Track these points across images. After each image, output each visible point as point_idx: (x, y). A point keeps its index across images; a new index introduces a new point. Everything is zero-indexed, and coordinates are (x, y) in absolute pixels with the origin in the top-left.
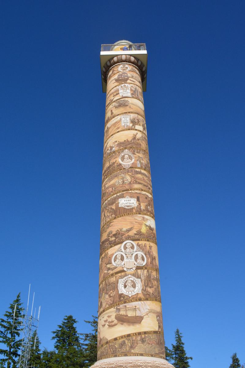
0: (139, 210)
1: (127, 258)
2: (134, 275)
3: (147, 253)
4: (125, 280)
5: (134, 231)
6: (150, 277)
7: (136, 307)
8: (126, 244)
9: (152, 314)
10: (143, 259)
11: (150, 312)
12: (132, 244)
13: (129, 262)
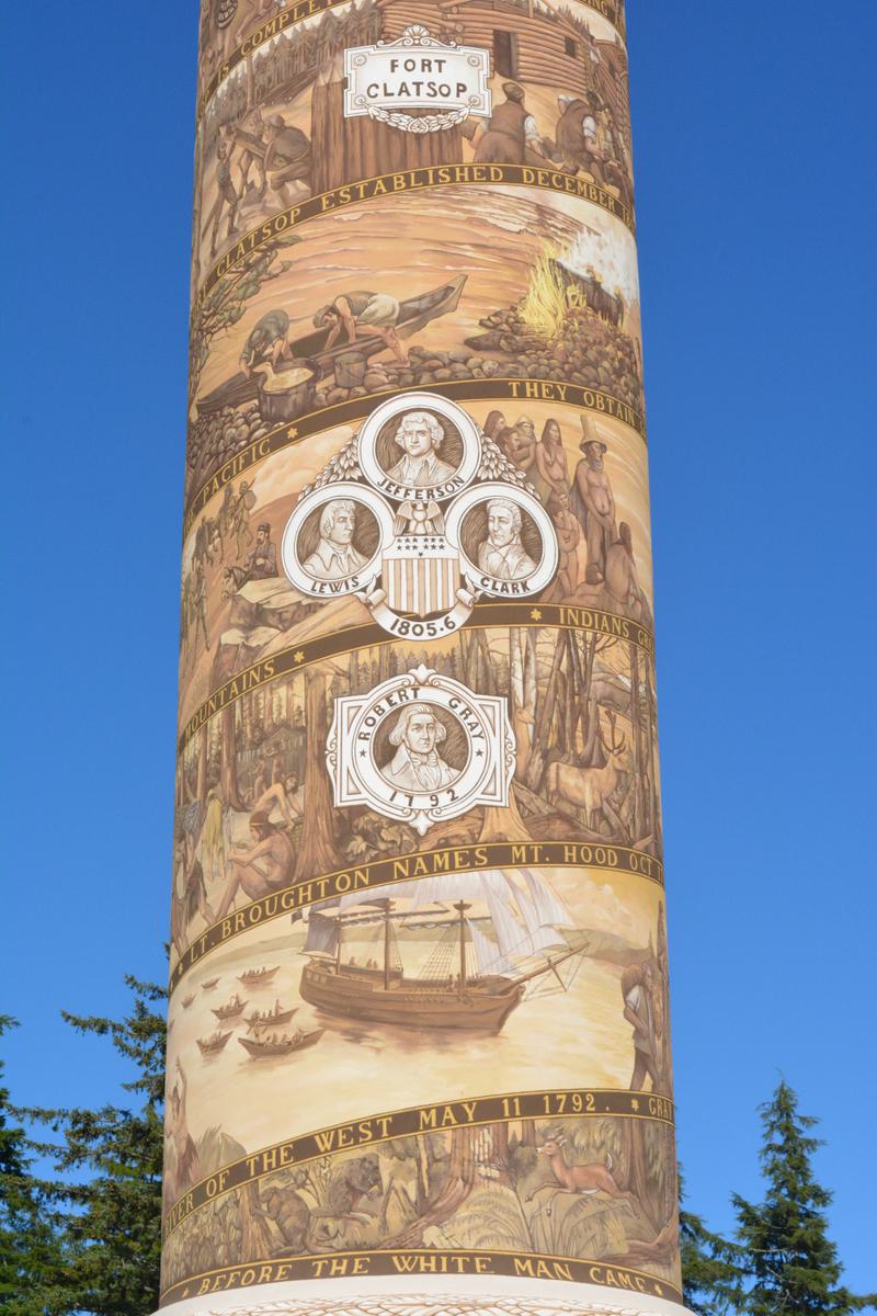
0: (510, 148)
1: (406, 530)
2: (453, 666)
3: (564, 499)
4: (384, 704)
5: (464, 321)
6: (584, 684)
7: (467, 913)
8: (396, 420)
9: (589, 962)
10: (531, 546)
11: (572, 951)
12: (442, 420)
13: (421, 568)
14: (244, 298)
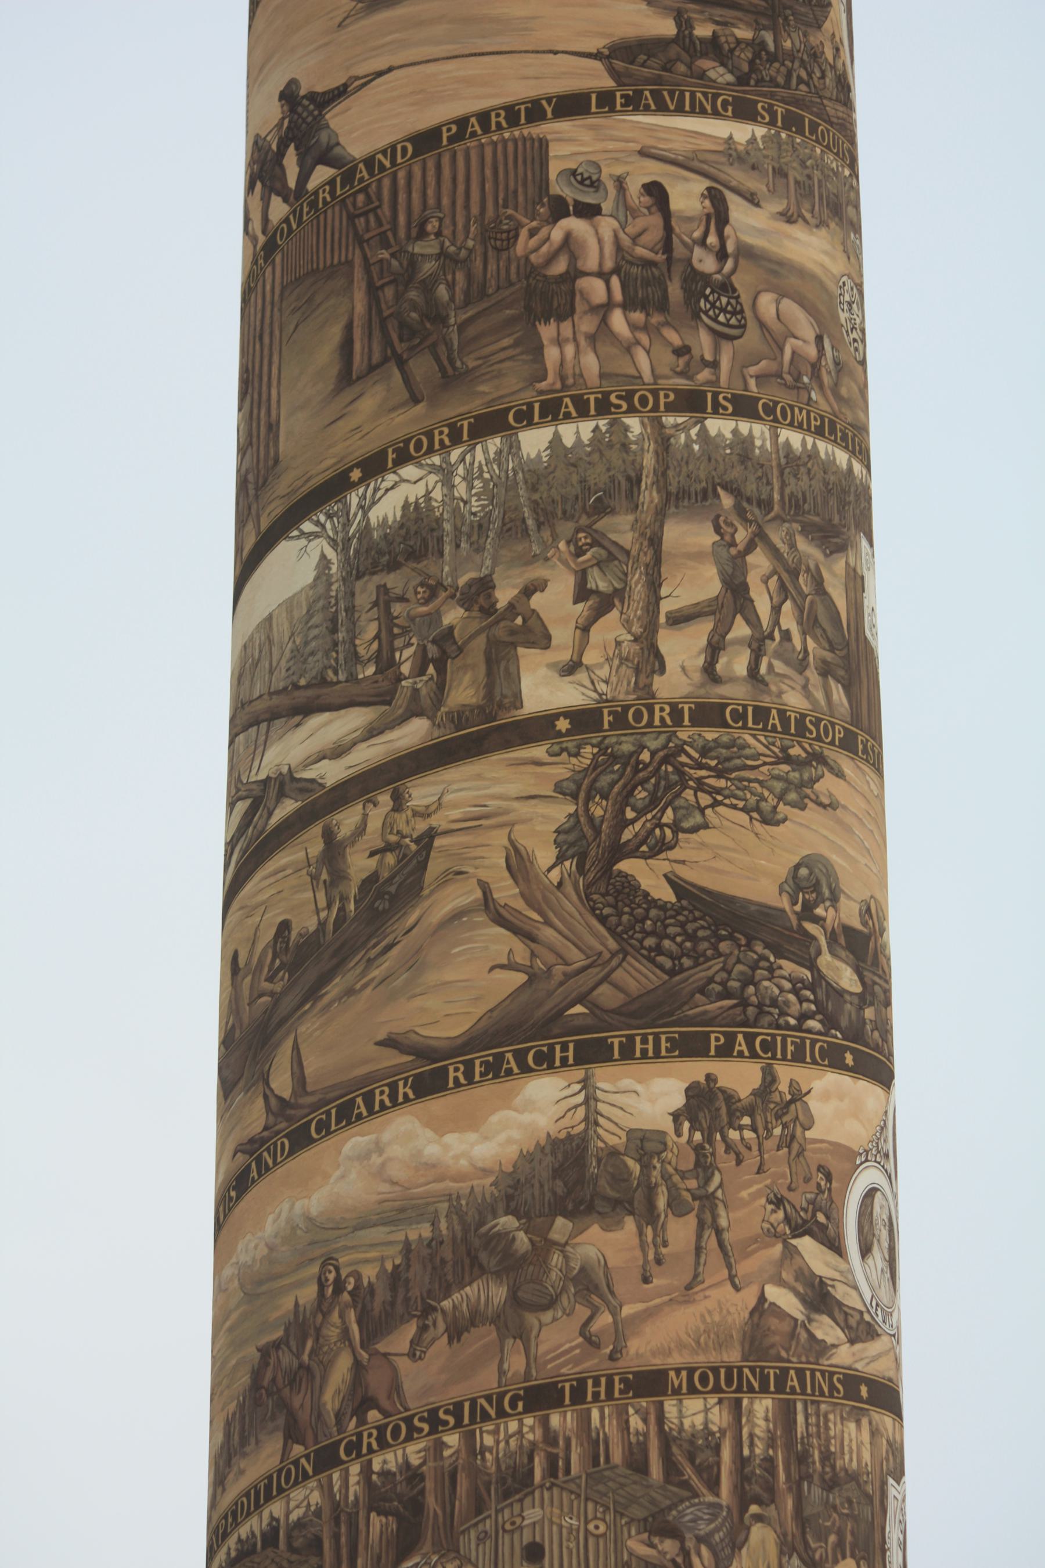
14: (781, 798)
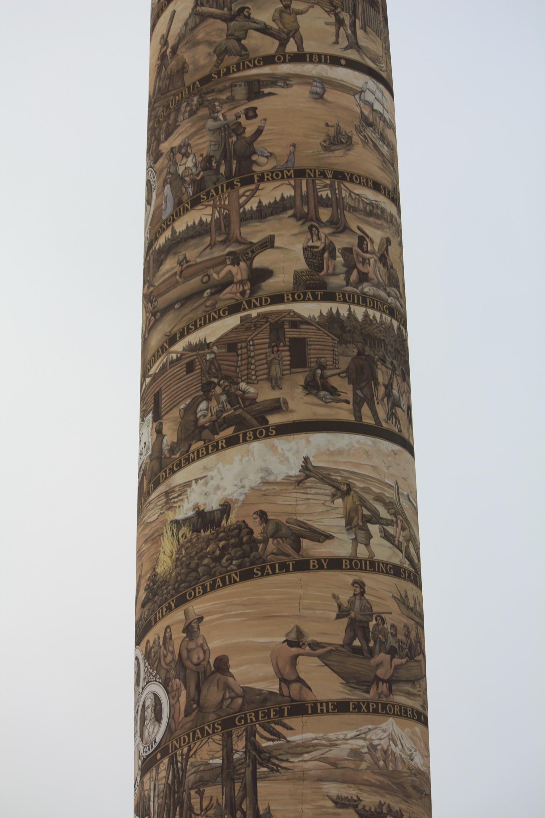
6: (181, 783)
